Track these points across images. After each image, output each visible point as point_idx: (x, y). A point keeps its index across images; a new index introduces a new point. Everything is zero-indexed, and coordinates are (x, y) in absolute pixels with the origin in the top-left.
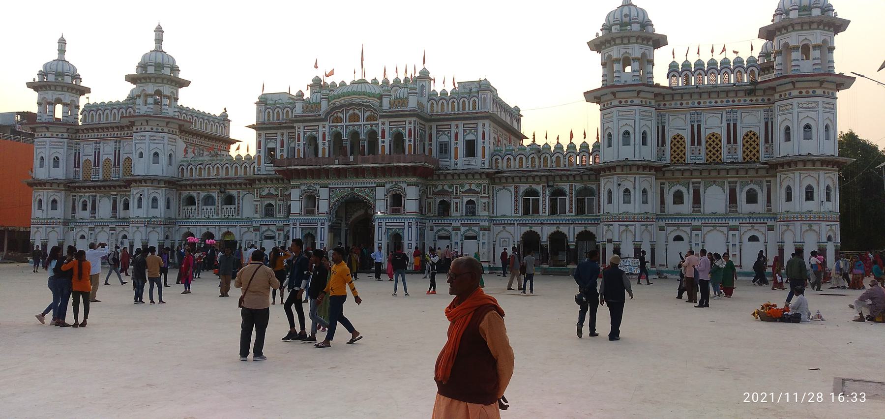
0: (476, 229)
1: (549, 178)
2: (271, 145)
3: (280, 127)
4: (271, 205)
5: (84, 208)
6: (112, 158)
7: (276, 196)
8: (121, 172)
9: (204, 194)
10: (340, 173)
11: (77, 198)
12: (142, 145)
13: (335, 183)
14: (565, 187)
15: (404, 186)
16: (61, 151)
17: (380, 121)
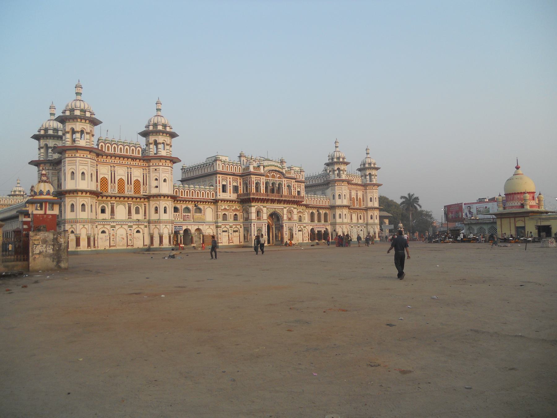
0: (302, 227)
1: (318, 208)
2: (224, 183)
3: (233, 175)
4: (224, 214)
5: (103, 211)
6: (125, 179)
7: (228, 210)
8: (133, 189)
9: (184, 206)
10: (273, 201)
11: (97, 204)
12: (167, 175)
13: (269, 205)
14: (321, 211)
15: (292, 208)
16: (93, 169)
17: (284, 179)
